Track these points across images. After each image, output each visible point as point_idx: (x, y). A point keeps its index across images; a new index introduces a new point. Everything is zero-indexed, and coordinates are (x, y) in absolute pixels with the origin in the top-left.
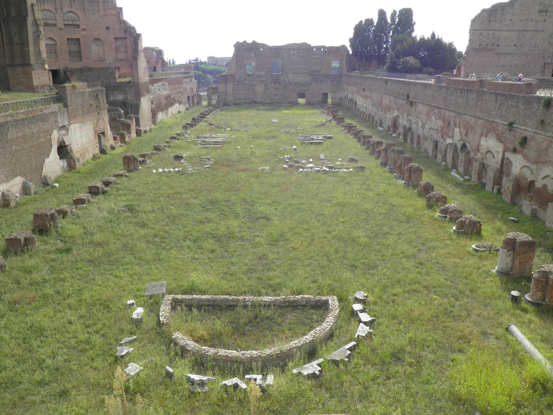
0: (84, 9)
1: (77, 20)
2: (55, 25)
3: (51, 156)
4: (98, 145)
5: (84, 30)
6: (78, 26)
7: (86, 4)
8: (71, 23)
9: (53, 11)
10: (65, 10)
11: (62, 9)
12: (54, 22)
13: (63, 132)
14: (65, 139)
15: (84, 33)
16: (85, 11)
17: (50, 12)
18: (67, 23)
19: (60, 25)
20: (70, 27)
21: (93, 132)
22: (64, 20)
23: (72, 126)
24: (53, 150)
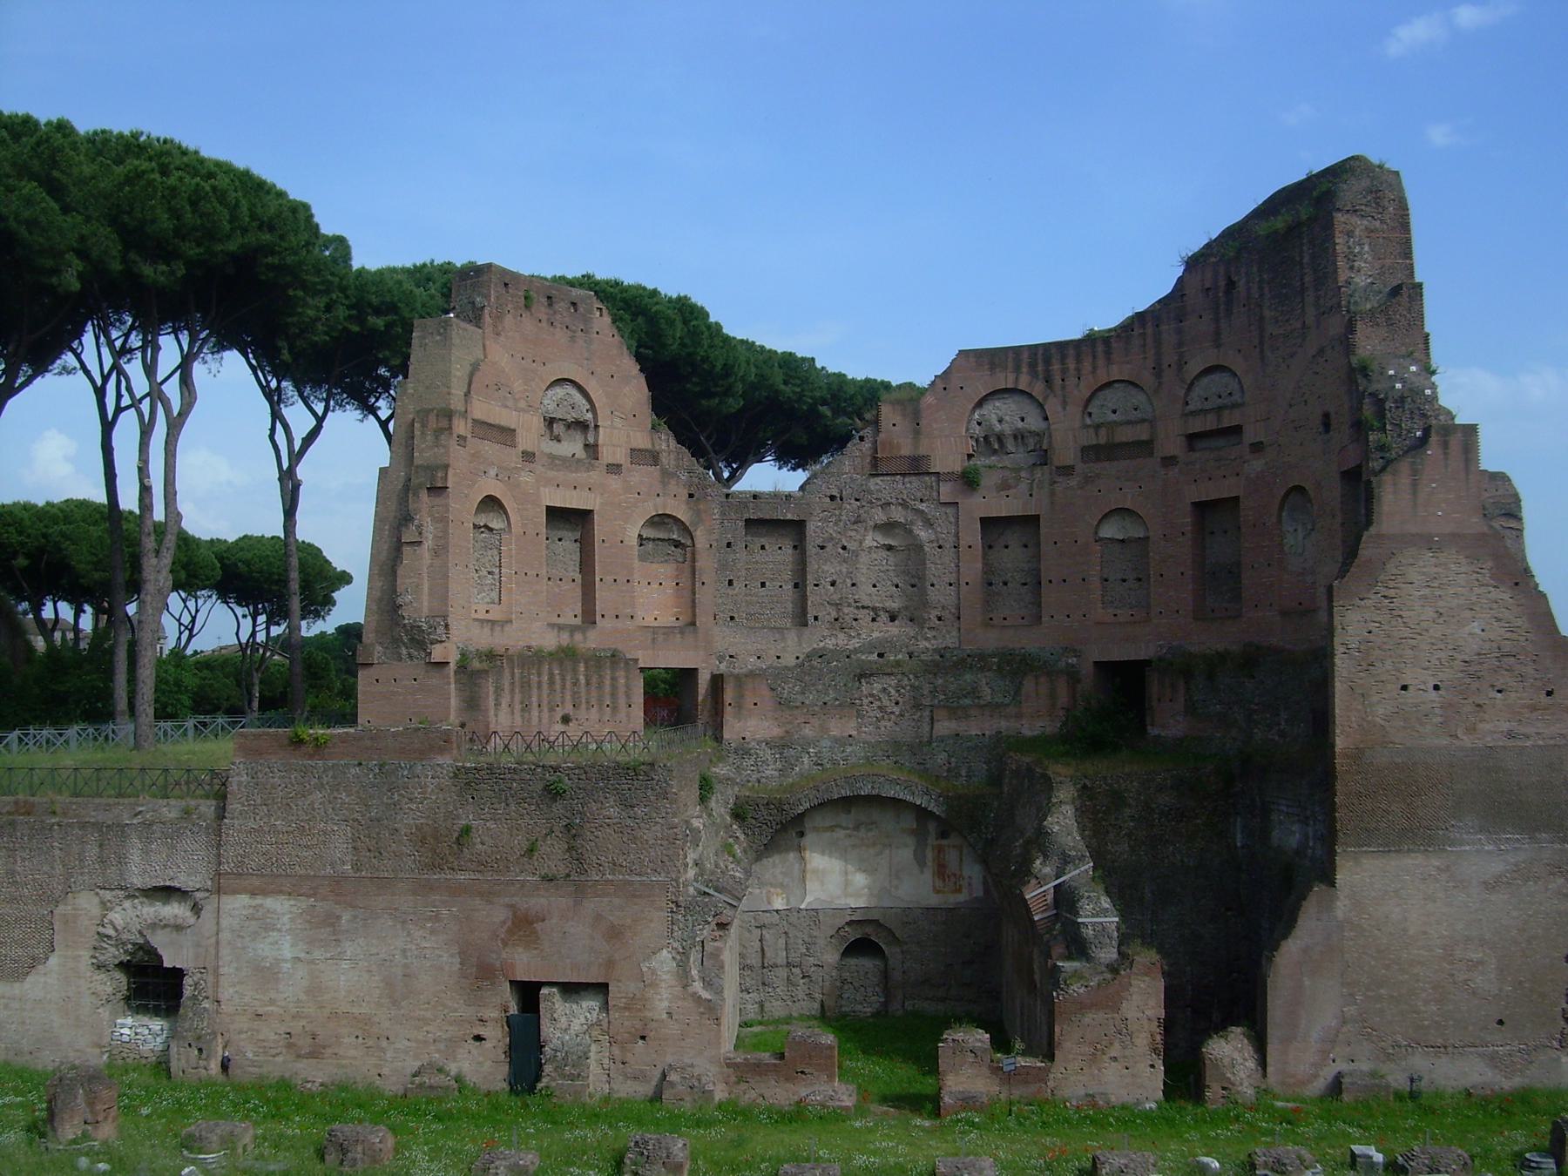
0: (1261, 343)
1: (1234, 406)
2: (1144, 447)
3: (30, 978)
4: (497, 1036)
5: (1257, 448)
6: (1237, 430)
7: (1267, 313)
8: (1210, 423)
9: (1147, 379)
10: (1195, 367)
11: (1181, 364)
12: (1143, 433)
13: (174, 910)
14: (158, 940)
15: (1256, 465)
16: (1262, 351)
17: (1134, 391)
18: (1197, 426)
19: (1171, 442)
20: (1221, 442)
21: (450, 961)
22: (1192, 413)
23: (237, 904)
24: (53, 960)
